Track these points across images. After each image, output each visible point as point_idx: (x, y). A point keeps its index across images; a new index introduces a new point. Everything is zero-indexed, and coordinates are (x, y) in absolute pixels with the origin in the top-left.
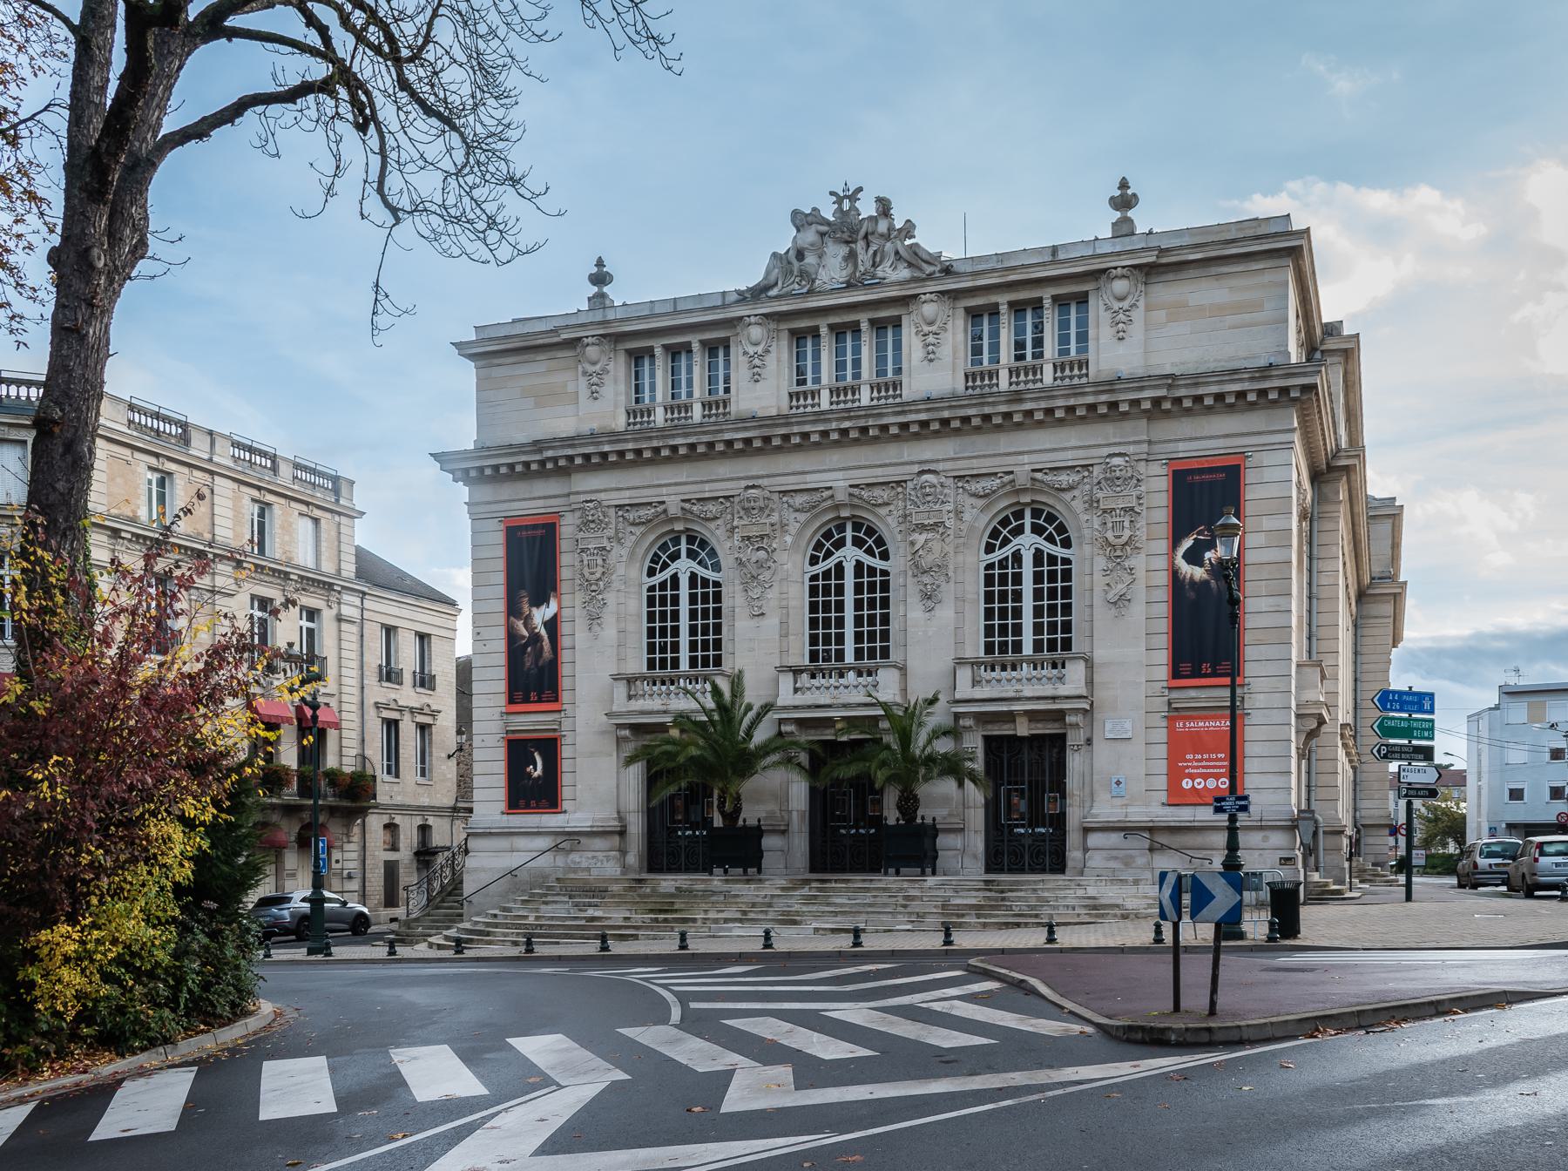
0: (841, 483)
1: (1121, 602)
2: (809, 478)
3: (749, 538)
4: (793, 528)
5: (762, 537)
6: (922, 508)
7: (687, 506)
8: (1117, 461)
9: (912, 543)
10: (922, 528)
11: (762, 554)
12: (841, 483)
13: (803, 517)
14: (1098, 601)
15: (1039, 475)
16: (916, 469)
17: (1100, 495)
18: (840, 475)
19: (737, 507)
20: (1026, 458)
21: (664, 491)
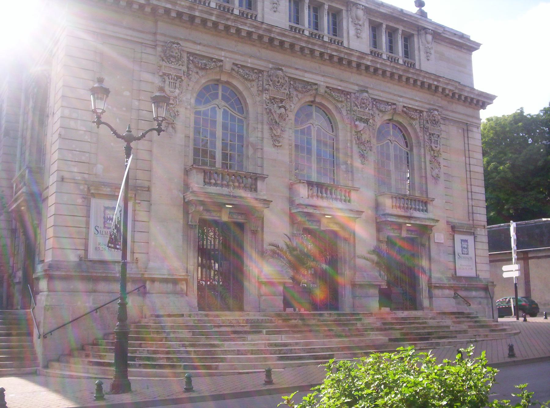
0: (322, 83)
1: (436, 178)
2: (306, 75)
3: (274, 98)
4: (295, 99)
5: (282, 101)
6: (360, 109)
7: (235, 68)
8: (436, 113)
9: (356, 126)
10: (361, 120)
11: (283, 110)
12: (322, 83)
13: (300, 96)
14: (429, 175)
15: (405, 109)
16: (356, 88)
17: (427, 125)
18: (322, 79)
19: (265, 77)
20: (401, 100)
21: (223, 53)
